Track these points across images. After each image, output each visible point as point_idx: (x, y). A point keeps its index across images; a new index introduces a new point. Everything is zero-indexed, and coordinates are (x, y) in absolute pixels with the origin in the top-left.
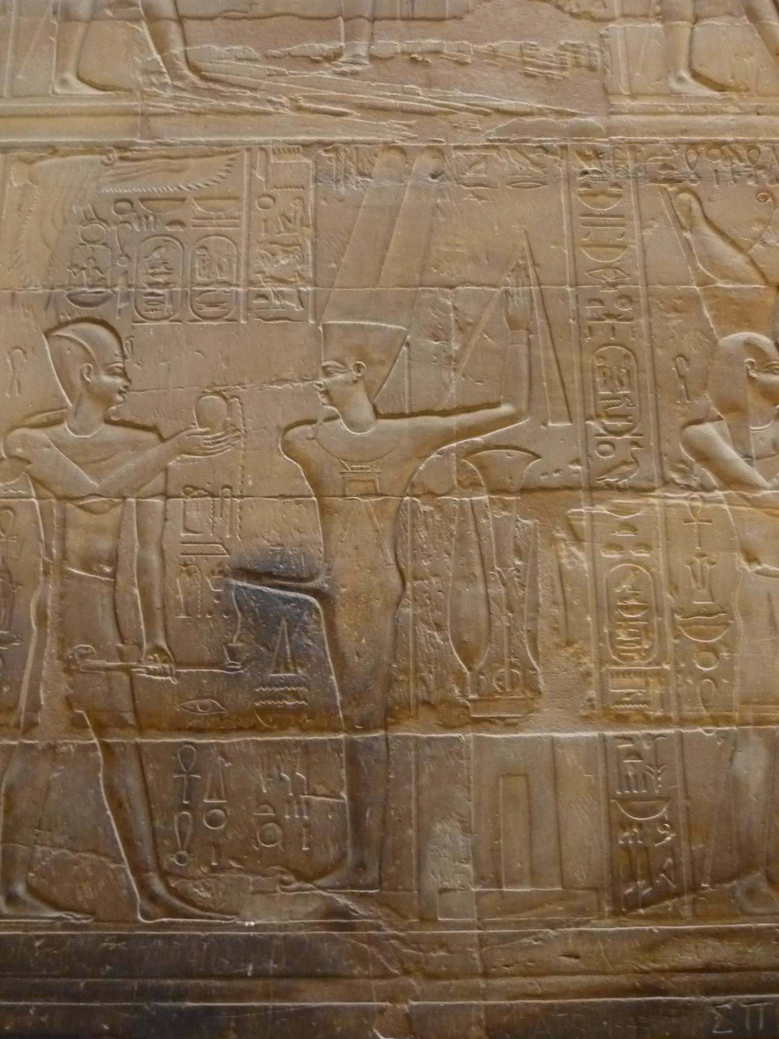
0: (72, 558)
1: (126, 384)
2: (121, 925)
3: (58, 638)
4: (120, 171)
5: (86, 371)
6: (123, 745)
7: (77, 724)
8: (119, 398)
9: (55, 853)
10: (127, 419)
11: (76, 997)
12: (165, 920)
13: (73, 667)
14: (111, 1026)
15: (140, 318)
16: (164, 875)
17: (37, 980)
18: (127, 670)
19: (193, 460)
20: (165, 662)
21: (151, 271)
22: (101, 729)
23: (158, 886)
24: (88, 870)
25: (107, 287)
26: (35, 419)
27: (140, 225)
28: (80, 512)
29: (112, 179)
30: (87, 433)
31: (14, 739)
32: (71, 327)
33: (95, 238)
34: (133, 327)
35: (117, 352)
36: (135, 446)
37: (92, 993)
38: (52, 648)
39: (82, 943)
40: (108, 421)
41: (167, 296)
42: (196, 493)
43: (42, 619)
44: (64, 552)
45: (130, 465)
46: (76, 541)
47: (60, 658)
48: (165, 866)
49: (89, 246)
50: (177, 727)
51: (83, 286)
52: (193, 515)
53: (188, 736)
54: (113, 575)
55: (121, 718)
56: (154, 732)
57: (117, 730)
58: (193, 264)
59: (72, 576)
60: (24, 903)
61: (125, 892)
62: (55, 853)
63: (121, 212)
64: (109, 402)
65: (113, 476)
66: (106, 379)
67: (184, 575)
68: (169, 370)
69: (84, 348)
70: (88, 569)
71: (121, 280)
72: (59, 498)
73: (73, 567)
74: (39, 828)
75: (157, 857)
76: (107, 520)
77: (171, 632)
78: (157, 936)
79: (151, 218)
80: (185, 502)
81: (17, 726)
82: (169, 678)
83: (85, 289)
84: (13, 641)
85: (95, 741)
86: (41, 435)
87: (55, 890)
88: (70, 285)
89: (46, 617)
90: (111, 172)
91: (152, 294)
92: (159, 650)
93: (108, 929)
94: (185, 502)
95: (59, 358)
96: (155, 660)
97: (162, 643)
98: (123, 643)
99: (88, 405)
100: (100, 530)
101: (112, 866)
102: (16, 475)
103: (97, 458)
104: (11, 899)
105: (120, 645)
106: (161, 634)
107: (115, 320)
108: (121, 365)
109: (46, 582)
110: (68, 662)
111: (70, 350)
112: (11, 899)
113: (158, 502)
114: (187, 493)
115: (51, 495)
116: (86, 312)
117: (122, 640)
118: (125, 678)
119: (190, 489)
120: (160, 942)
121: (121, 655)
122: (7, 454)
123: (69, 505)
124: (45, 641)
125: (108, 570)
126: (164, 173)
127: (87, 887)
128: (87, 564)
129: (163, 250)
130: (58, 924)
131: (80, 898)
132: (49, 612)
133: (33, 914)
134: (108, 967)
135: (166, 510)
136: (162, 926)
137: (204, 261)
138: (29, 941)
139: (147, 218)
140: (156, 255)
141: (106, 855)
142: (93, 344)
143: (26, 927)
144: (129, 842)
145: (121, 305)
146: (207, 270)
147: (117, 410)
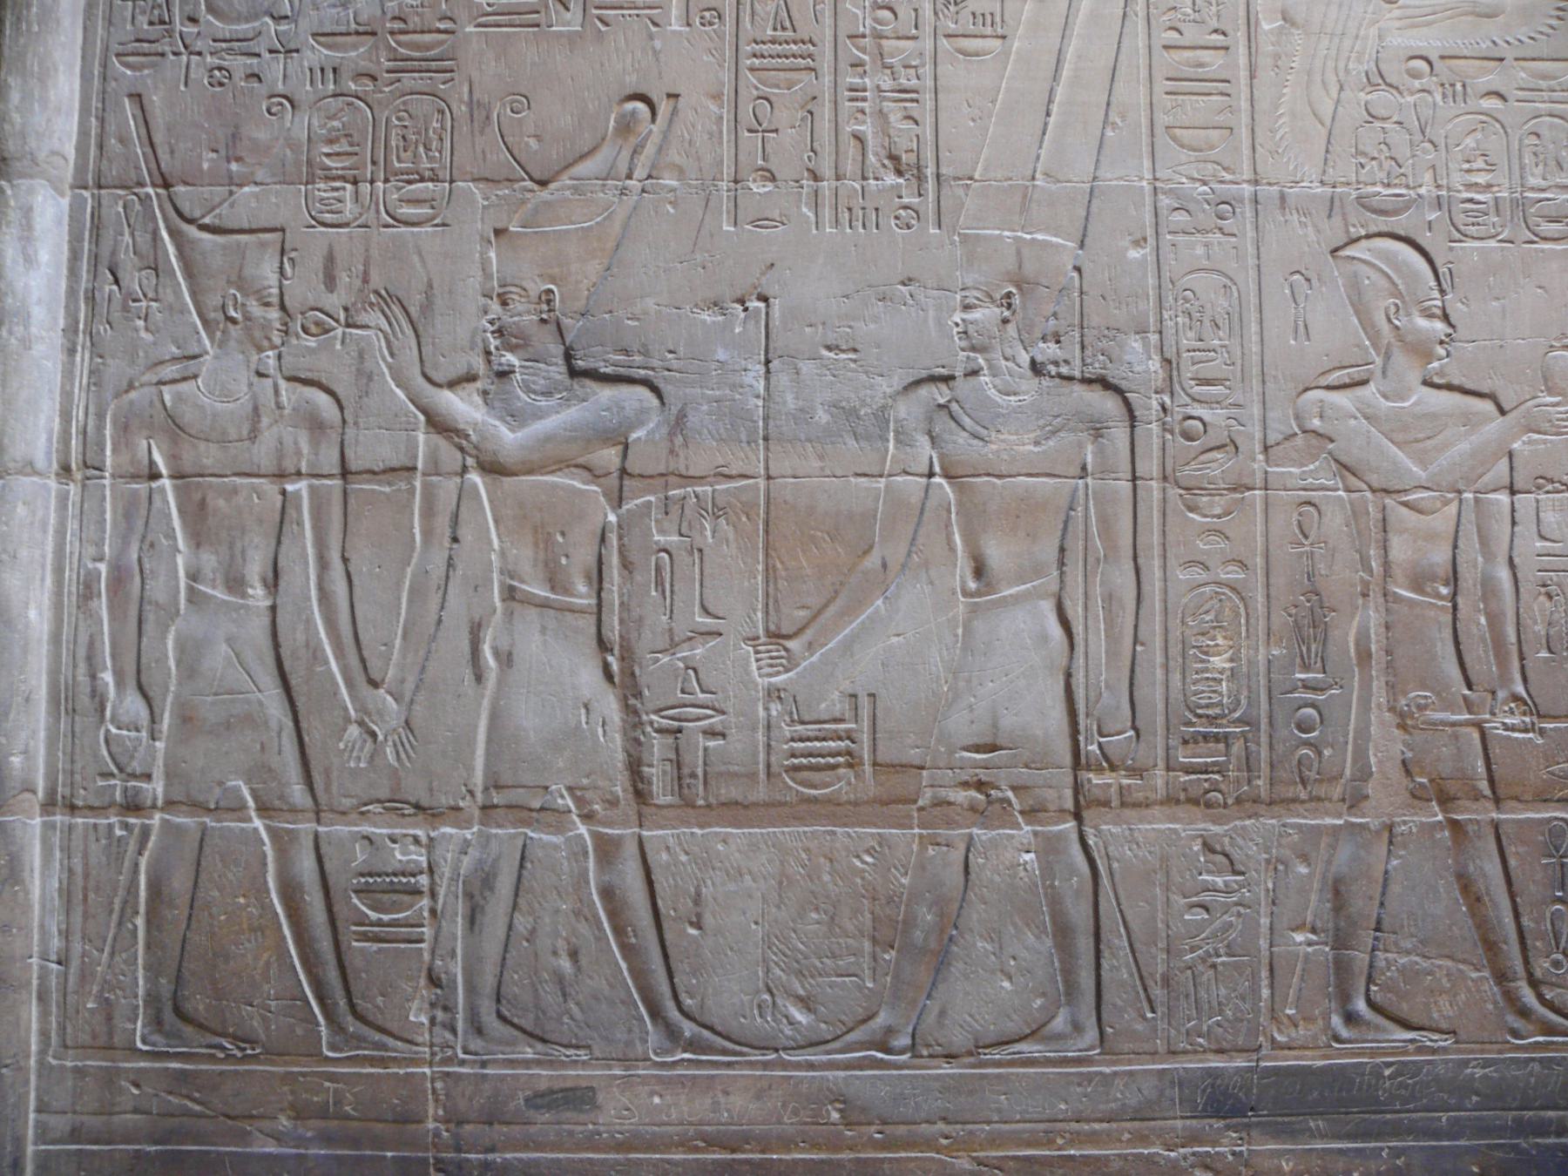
0: (1397, 572)
1: (1450, 331)
2: (1487, 1046)
3: (1387, 683)
4: (1409, 12)
5: (1393, 309)
6: (1478, 822)
7: (1417, 795)
8: (1441, 351)
9: (1403, 960)
10: (1456, 382)
11: (1436, 1134)
12: (1541, 1039)
13: (1409, 722)
14: (1481, 1168)
15: (1457, 236)
16: (1534, 983)
17: (1389, 1116)
18: (1479, 725)
19: (1545, 442)
20: (1524, 714)
21: (1466, 166)
22: (1445, 800)
23: (1528, 997)
24: (1444, 981)
25: (1407, 187)
26: (1332, 378)
27: (1444, 96)
28: (1404, 510)
29: (1398, 24)
30: (1403, 399)
31: (1339, 816)
32: (1364, 243)
33: (1383, 113)
34: (1451, 249)
35: (1433, 283)
36: (1470, 421)
37: (1455, 1130)
38: (1379, 696)
39: (1441, 1069)
40: (1427, 383)
41: (1492, 203)
42: (1550, 487)
43: (1364, 656)
44: (1386, 564)
45: (1464, 446)
46: (1400, 550)
47: (1392, 709)
48: (1538, 974)
49: (1378, 124)
50: (1544, 800)
51: (1374, 184)
52: (1549, 517)
53: (1556, 809)
54: (1453, 597)
55: (1474, 788)
56: (1514, 804)
57: (1468, 803)
58: (1520, 157)
59: (1398, 599)
60: (1368, 1024)
61: (1490, 1007)
62: (1403, 960)
63: (1415, 75)
64: (1429, 356)
65: (1443, 460)
66: (1422, 323)
67: (1542, 598)
68: (1504, 311)
69: (1389, 277)
70: (1418, 589)
71: (1428, 176)
72: (1373, 491)
73: (1400, 587)
74: (1377, 930)
75: (1526, 962)
76: (1443, 520)
77: (1530, 674)
78: (1533, 1059)
79: (1459, 87)
80: (1537, 501)
81: (1343, 800)
82: (1531, 735)
83: (1379, 189)
84: (1331, 687)
85: (1440, 817)
86: (1341, 399)
87: (1405, 1006)
88: (1358, 182)
89: (1370, 655)
90: (1397, 13)
91: (1471, 201)
92: (1516, 698)
93: (1472, 1052)
94: (1537, 501)
95: (1354, 286)
96: (1512, 712)
97: (1520, 689)
98: (1470, 687)
99: (1400, 359)
100: (1432, 537)
101: (1474, 975)
102: (1315, 458)
103: (1421, 436)
104: (1350, 1018)
105: (1467, 692)
106: (1517, 676)
107: (1425, 239)
108: (1439, 303)
109: (1365, 607)
110: (1402, 715)
111: (1369, 278)
112: (1350, 1018)
113: (1504, 497)
114: (1539, 488)
115: (1365, 487)
116: (1382, 224)
117: (1470, 687)
118: (1476, 735)
119: (1543, 481)
120: (1537, 1067)
121: (1469, 706)
122: (1299, 426)
123: (1388, 501)
124: (1370, 687)
125: (1444, 591)
126: (1470, 18)
127: (1444, 1002)
128: (1417, 585)
129: (1479, 135)
130: (1411, 1047)
131: (1435, 1015)
132: (1373, 648)
133: (1380, 1036)
134: (1475, 1098)
135: (1513, 511)
136: (1537, 1046)
137: (1535, 154)
138: (1377, 1071)
139: (1452, 85)
140: (1470, 142)
141: (1464, 962)
142: (1397, 269)
143: (1373, 1053)
144: (1491, 947)
145: (1432, 216)
146: (1541, 167)
147: (1442, 366)
